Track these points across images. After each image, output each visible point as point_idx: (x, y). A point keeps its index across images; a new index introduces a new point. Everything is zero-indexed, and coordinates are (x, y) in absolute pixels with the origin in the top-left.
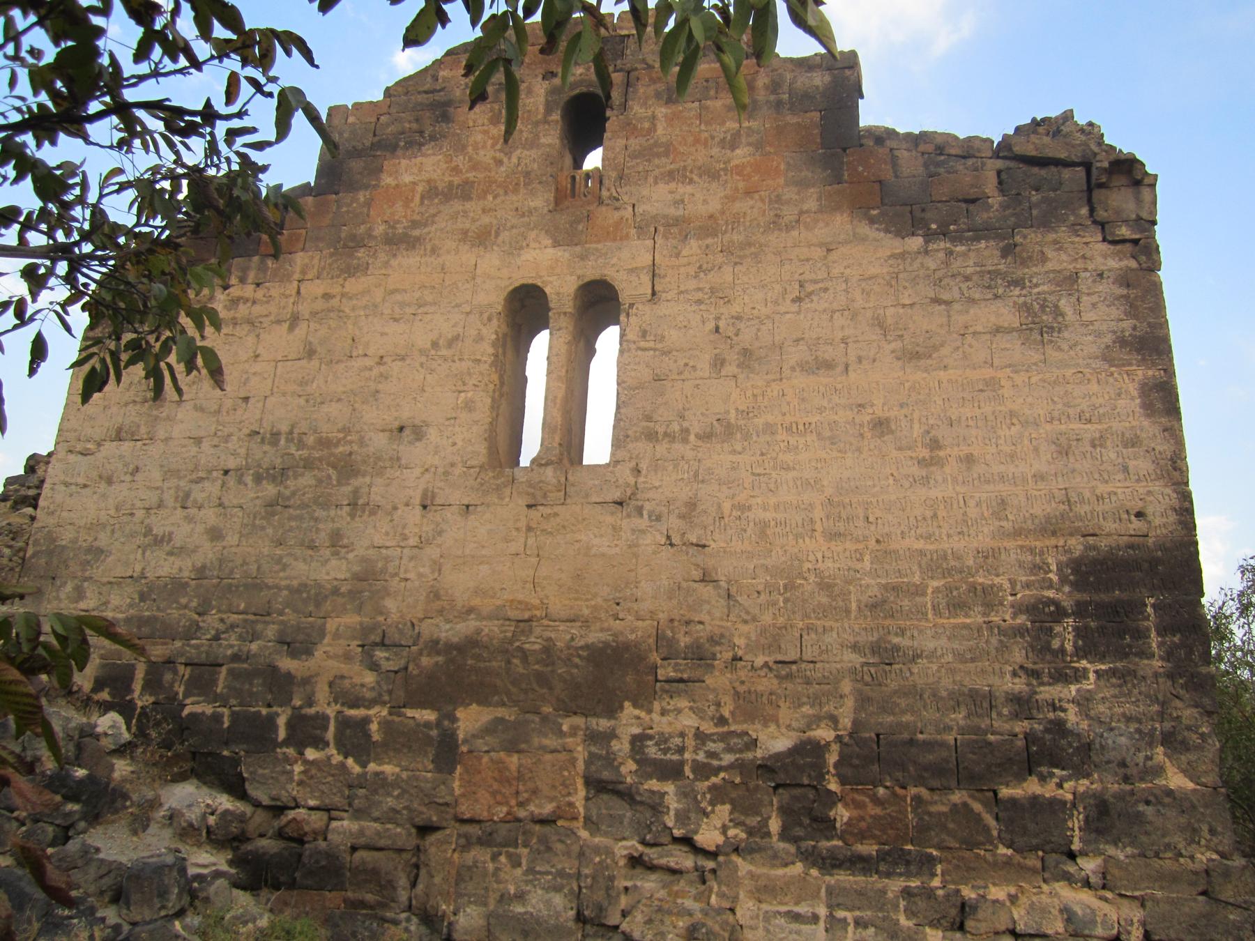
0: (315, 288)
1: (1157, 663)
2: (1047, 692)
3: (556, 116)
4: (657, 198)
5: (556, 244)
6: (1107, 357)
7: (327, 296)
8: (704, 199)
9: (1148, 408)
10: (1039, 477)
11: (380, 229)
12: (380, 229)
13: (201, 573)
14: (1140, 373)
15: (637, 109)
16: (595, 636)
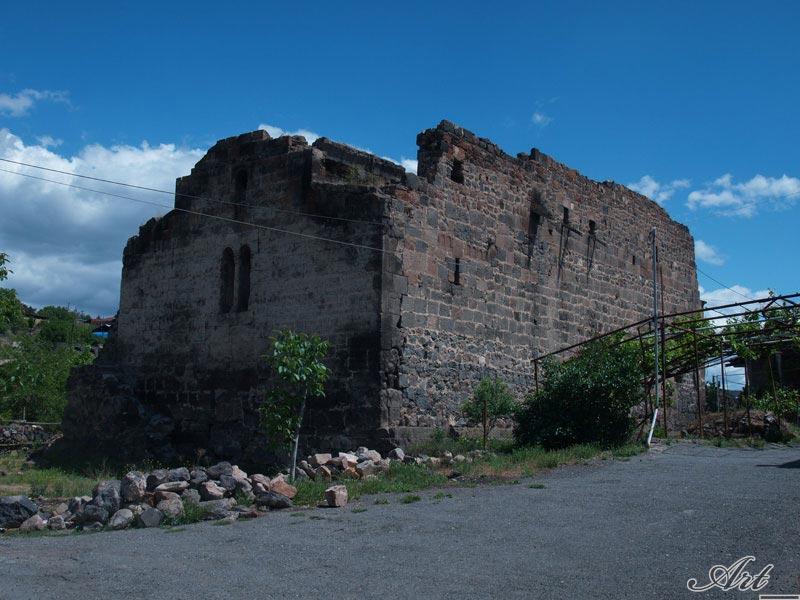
0: (176, 252)
1: (367, 370)
2: (343, 380)
3: (234, 181)
4: (259, 212)
5: (235, 232)
6: (366, 268)
7: (180, 254)
8: (271, 212)
9: (375, 287)
10: (346, 311)
11: (192, 228)
12: (192, 228)
13: (156, 350)
14: (374, 273)
15: (255, 178)
16: (244, 367)
